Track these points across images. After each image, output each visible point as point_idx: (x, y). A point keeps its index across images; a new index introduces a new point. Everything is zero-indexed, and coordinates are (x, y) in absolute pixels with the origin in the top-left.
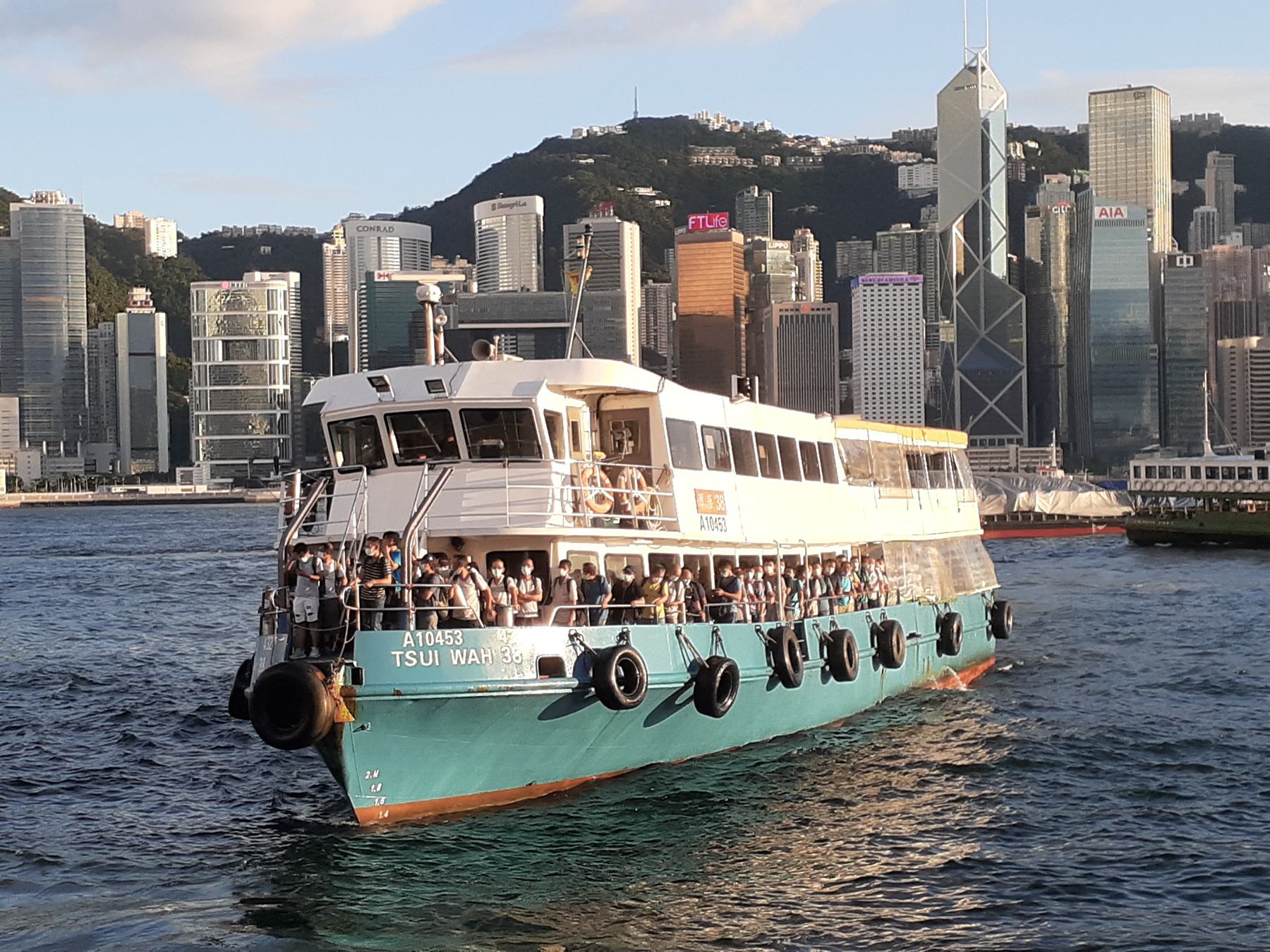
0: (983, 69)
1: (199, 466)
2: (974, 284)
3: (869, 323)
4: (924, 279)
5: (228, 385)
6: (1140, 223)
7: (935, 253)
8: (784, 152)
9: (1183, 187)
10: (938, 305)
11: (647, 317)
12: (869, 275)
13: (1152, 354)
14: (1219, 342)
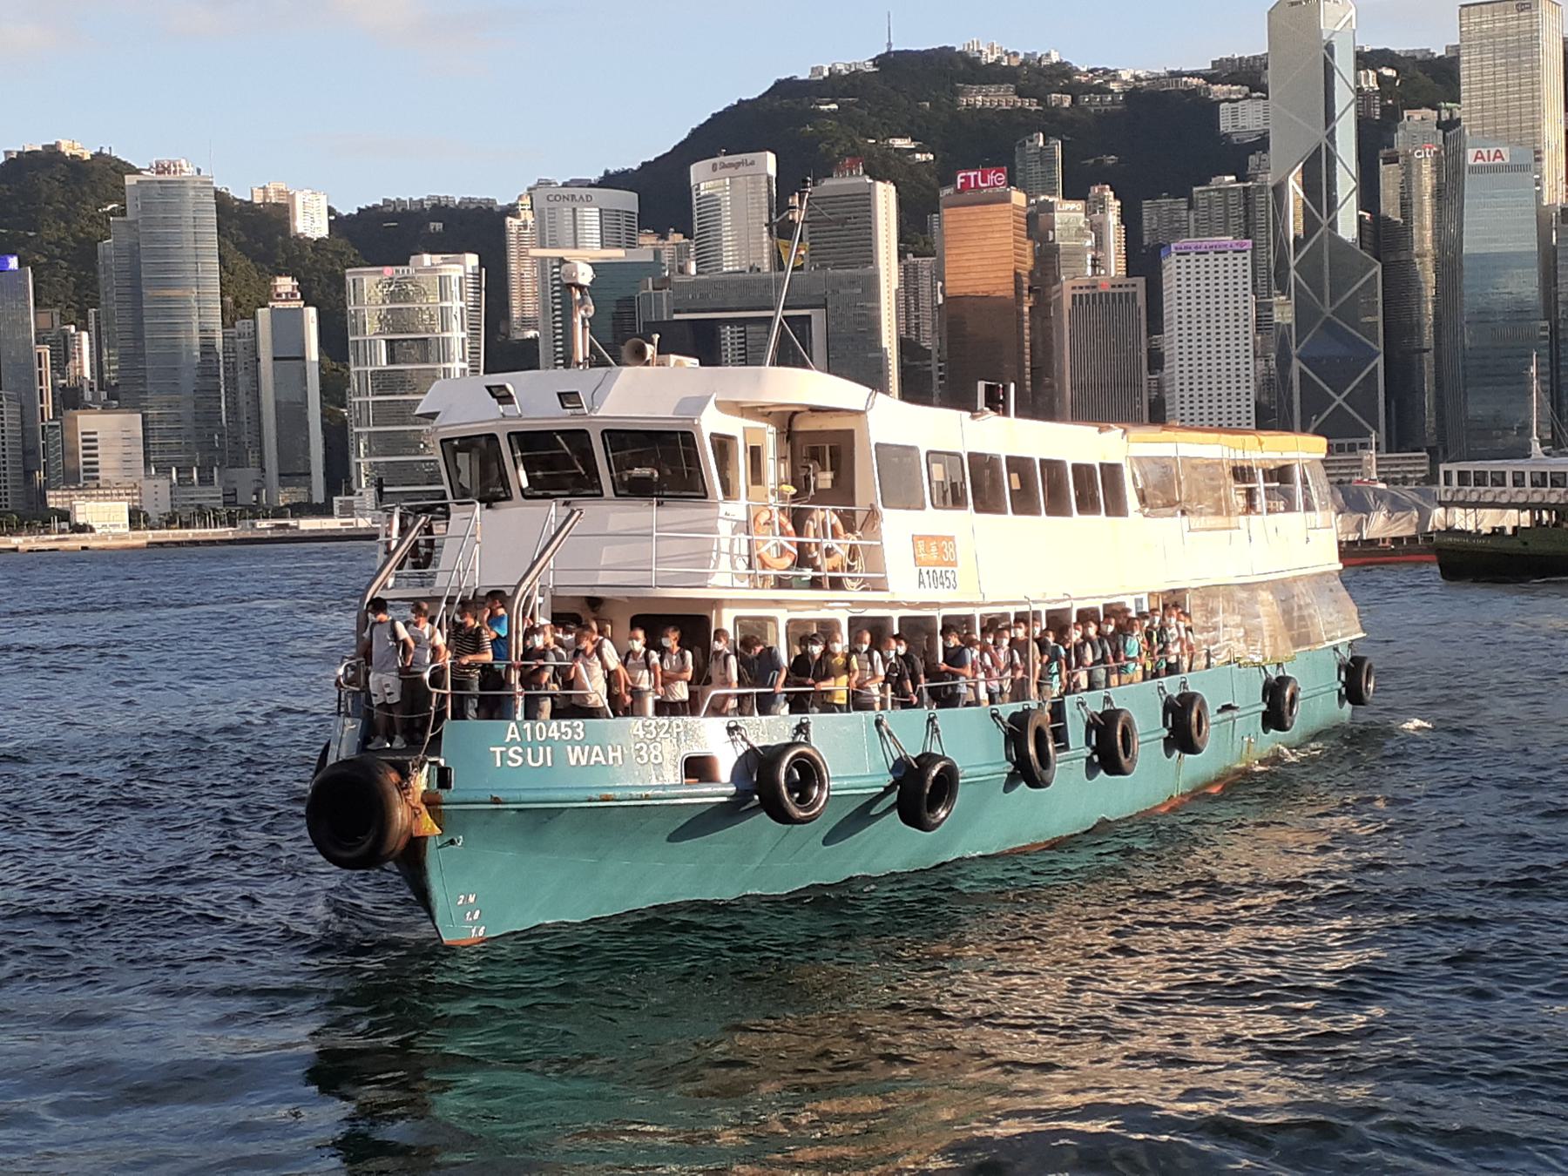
1: (361, 494)
2: (1316, 251)
3: (1184, 301)
4: (1254, 244)
5: (394, 394)
7: (1267, 211)
8: (1076, 90)
11: (907, 300)
12: (1183, 242)
13: (1542, 333)
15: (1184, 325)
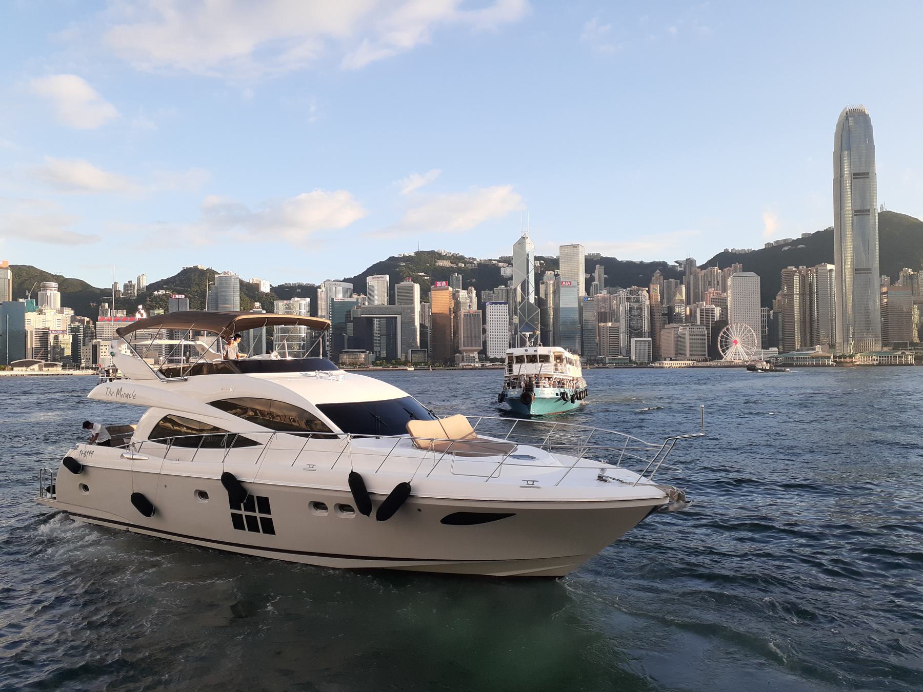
0: (527, 238)
2: (524, 307)
3: (491, 316)
6: (576, 287)
9: (589, 276)
10: (513, 312)
15: (492, 323)
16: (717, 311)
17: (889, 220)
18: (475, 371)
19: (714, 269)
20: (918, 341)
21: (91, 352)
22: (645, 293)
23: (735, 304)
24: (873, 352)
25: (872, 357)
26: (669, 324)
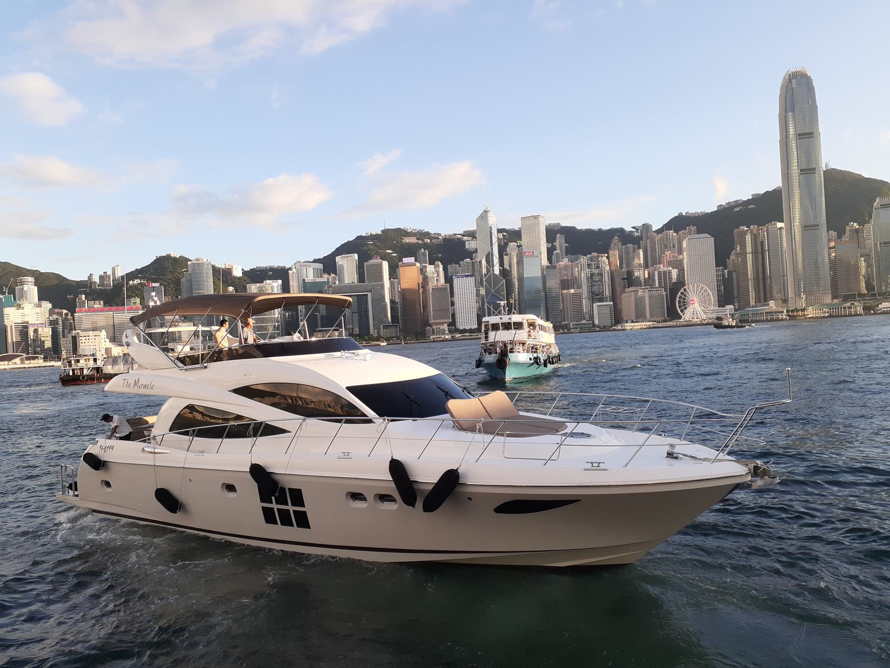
0: (489, 211)
3: (459, 289)
6: (537, 256)
8: (431, 238)
9: (550, 245)
14: (563, 291)
16: (675, 273)
17: (834, 177)
18: (445, 342)
19: (670, 232)
20: (866, 292)
21: (71, 344)
22: (605, 259)
23: (691, 265)
24: (823, 305)
25: (823, 310)
26: (629, 287)
